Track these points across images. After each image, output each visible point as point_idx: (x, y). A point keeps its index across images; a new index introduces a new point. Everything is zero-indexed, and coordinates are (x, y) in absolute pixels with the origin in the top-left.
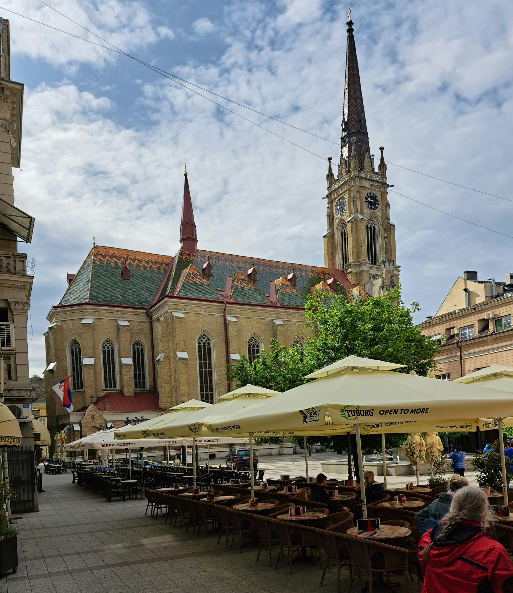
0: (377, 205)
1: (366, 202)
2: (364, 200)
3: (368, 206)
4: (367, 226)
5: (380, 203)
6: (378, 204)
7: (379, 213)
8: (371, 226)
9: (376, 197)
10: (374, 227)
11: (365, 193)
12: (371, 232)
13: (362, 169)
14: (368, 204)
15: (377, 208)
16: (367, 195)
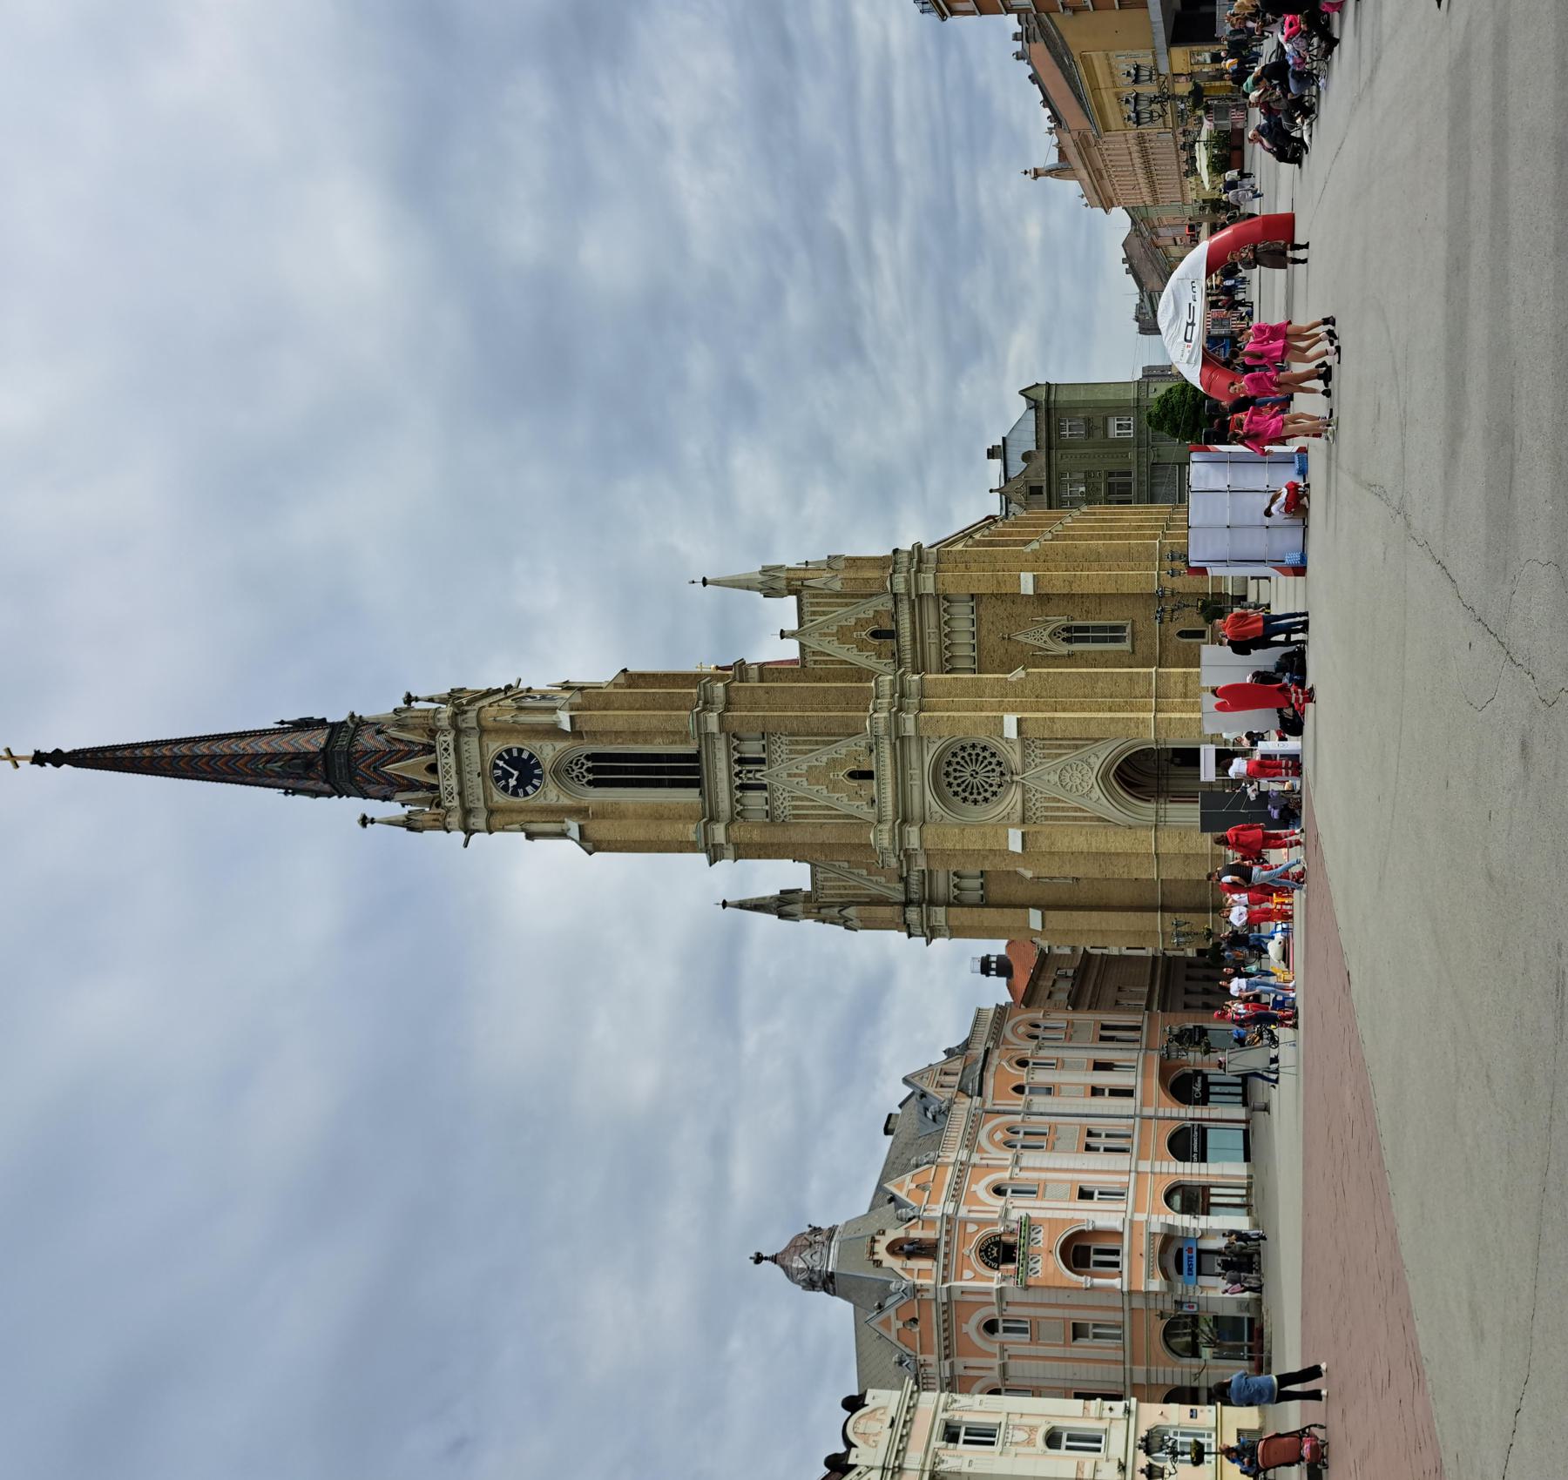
0: (525, 756)
1: (526, 794)
2: (519, 801)
3: (536, 788)
4: (590, 783)
5: (514, 744)
6: (520, 751)
7: (548, 752)
8: (589, 770)
9: (500, 757)
10: (588, 758)
11: (500, 799)
12: (610, 770)
13: (435, 788)
14: (529, 789)
15: (531, 756)
16: (505, 788)
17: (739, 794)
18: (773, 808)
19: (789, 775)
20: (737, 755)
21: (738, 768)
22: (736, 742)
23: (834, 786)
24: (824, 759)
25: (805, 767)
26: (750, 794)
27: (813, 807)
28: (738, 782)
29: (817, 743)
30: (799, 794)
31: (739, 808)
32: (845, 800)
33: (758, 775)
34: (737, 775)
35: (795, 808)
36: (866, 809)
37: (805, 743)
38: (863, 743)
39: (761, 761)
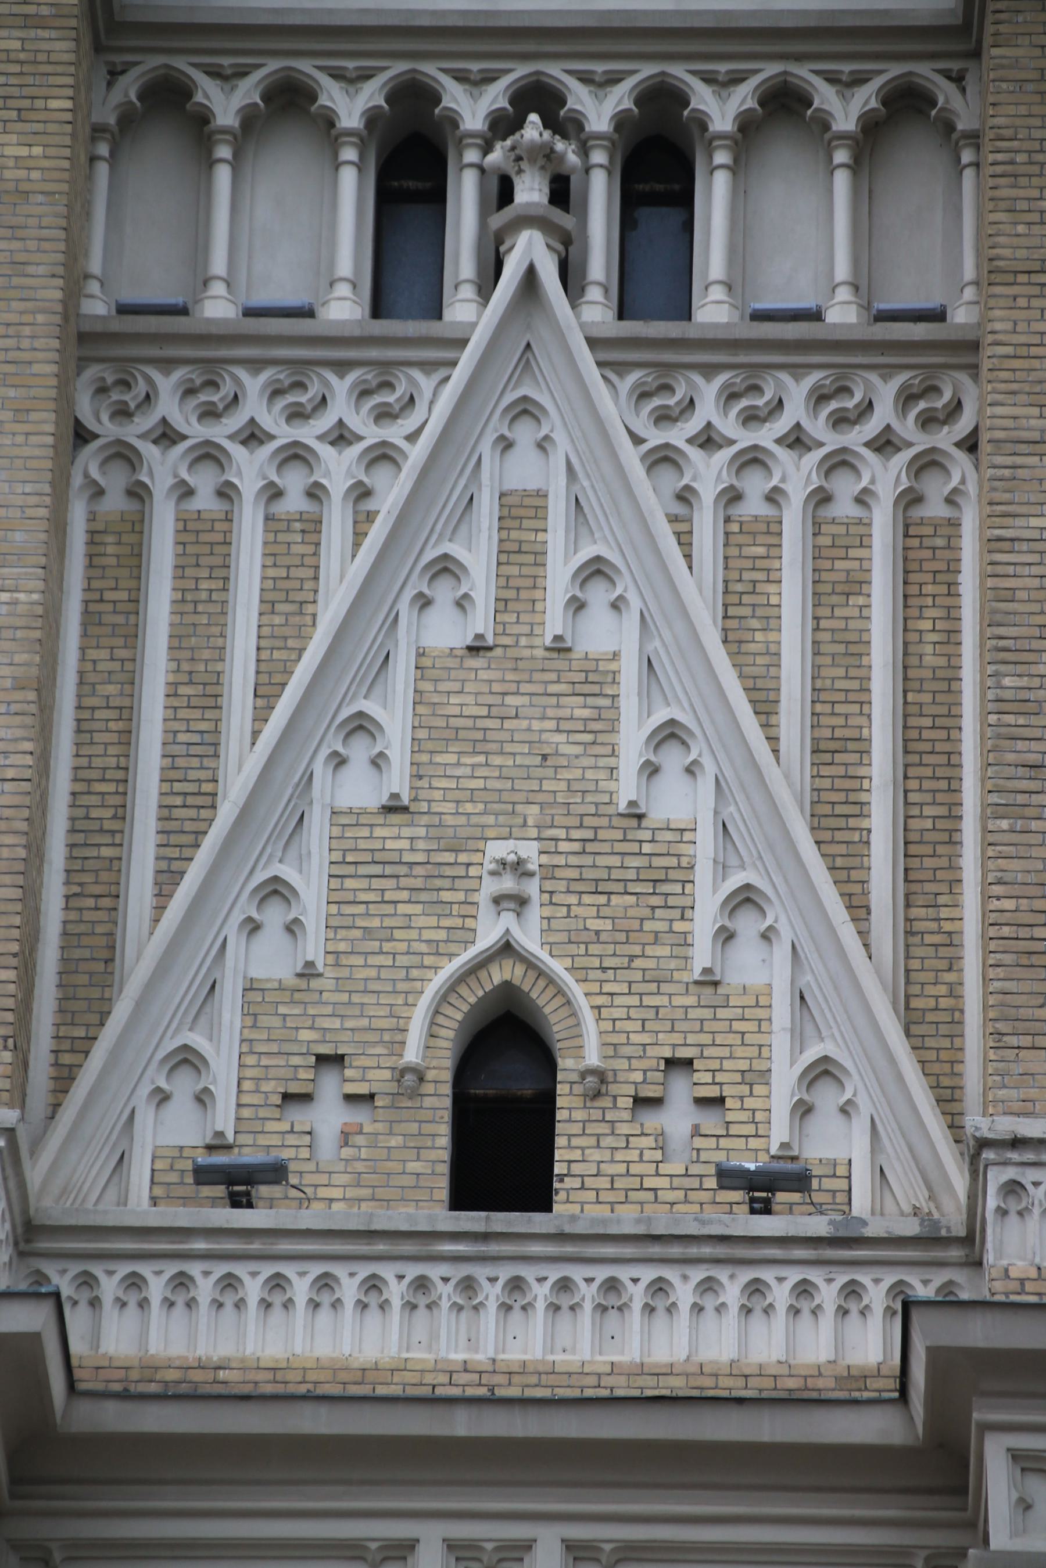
17: (351, 107)
18: (214, 360)
19: (521, 512)
20: (720, 110)
21: (600, 111)
22: (845, 111)
23: (400, 863)
24: (676, 801)
25: (602, 634)
26: (351, 192)
27: (199, 692)
28: (472, 109)
29: (835, 749)
30: (341, 574)
31: (225, 105)
32: (271, 960)
33: (529, 249)
34: (539, 98)
35: (206, 550)
36: (179, 1129)
37: (838, 650)
38: (836, 1143)
39: (654, 276)
